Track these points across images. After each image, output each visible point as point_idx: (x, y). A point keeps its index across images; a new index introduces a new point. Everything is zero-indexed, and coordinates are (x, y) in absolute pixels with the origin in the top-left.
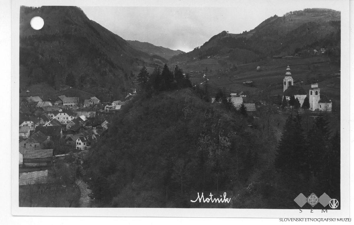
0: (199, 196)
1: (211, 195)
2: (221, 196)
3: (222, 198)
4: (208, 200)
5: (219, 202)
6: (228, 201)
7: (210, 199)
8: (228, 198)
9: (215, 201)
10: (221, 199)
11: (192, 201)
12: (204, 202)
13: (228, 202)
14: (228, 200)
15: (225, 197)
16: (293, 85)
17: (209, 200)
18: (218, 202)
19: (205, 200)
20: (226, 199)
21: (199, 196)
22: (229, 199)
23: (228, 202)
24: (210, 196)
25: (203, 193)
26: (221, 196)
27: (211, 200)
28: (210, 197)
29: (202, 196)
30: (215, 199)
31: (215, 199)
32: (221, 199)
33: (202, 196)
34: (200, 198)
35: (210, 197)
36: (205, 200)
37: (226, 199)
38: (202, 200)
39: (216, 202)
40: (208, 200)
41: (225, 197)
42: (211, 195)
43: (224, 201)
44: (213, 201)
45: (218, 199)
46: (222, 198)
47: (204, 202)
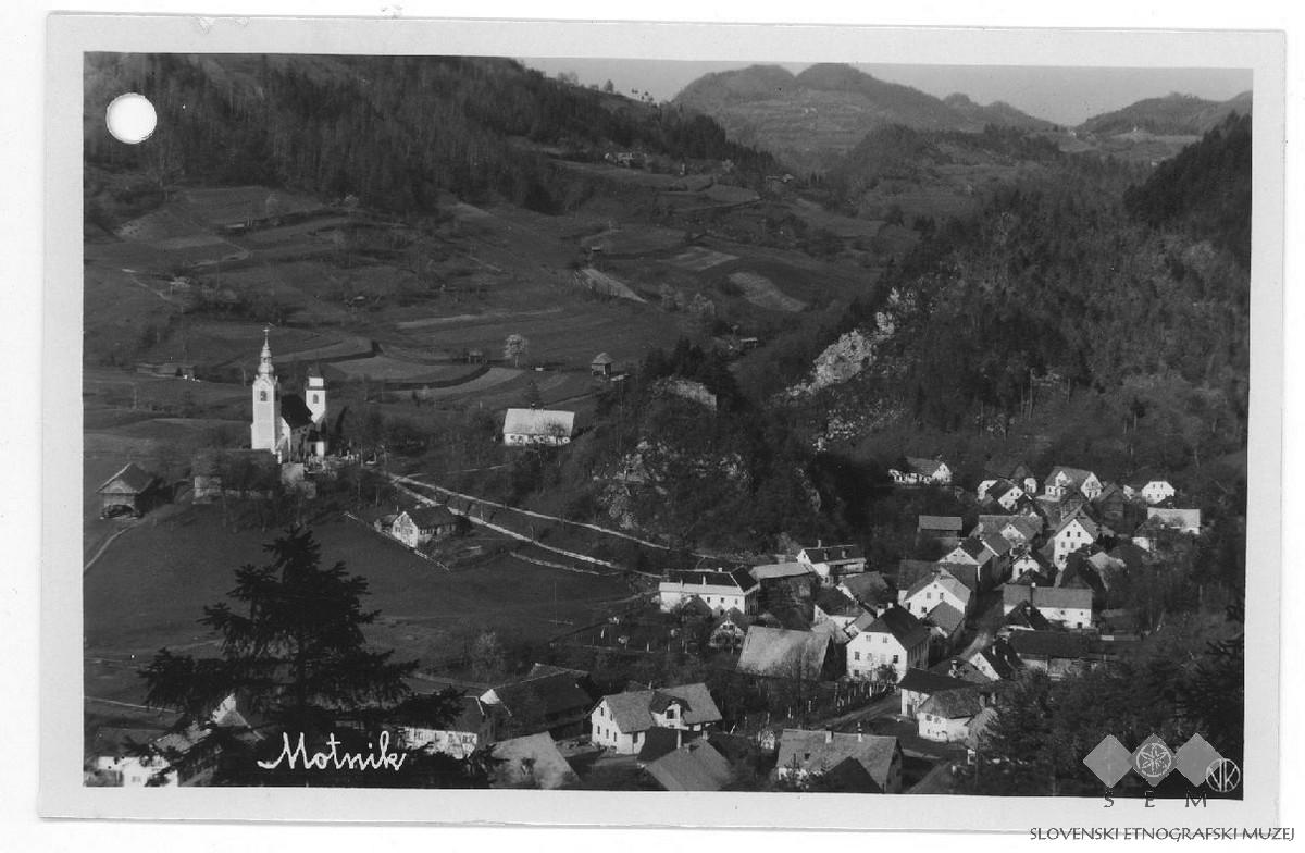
0: (287, 749)
1: (333, 743)
2: (370, 746)
3: (372, 755)
4: (320, 760)
5: (363, 767)
6: (397, 763)
7: (312, 763)
8: (395, 755)
9: (347, 763)
10: (371, 757)
11: (260, 763)
12: (308, 766)
13: (397, 768)
14: (396, 758)
15: (384, 749)
16: (567, 419)
17: (326, 759)
18: (359, 766)
19: (309, 760)
20: (387, 755)
21: (287, 749)
22: (399, 758)
23: (397, 768)
24: (328, 743)
25: (302, 735)
26: (370, 746)
27: (331, 762)
28: (328, 750)
29: (301, 745)
30: (347, 756)
31: (347, 756)
32: (371, 757)
33: (301, 745)
34: (292, 753)
35: (328, 750)
36: (309, 760)
37: (387, 755)
38: (300, 760)
39: (351, 767)
40: (320, 760)
41: (384, 749)
42: (333, 743)
43: (380, 763)
44: (340, 763)
45: (359, 756)
46: (372, 755)
47: (308, 766)
